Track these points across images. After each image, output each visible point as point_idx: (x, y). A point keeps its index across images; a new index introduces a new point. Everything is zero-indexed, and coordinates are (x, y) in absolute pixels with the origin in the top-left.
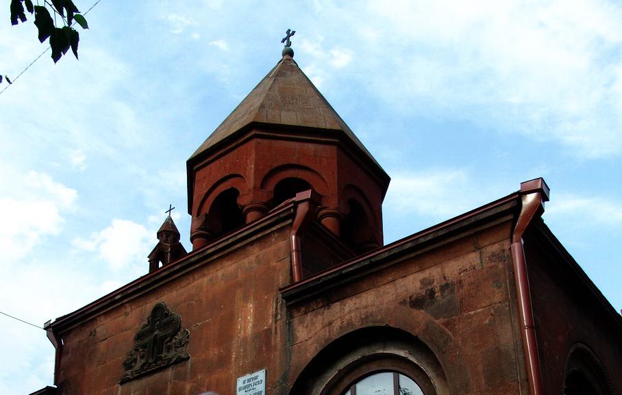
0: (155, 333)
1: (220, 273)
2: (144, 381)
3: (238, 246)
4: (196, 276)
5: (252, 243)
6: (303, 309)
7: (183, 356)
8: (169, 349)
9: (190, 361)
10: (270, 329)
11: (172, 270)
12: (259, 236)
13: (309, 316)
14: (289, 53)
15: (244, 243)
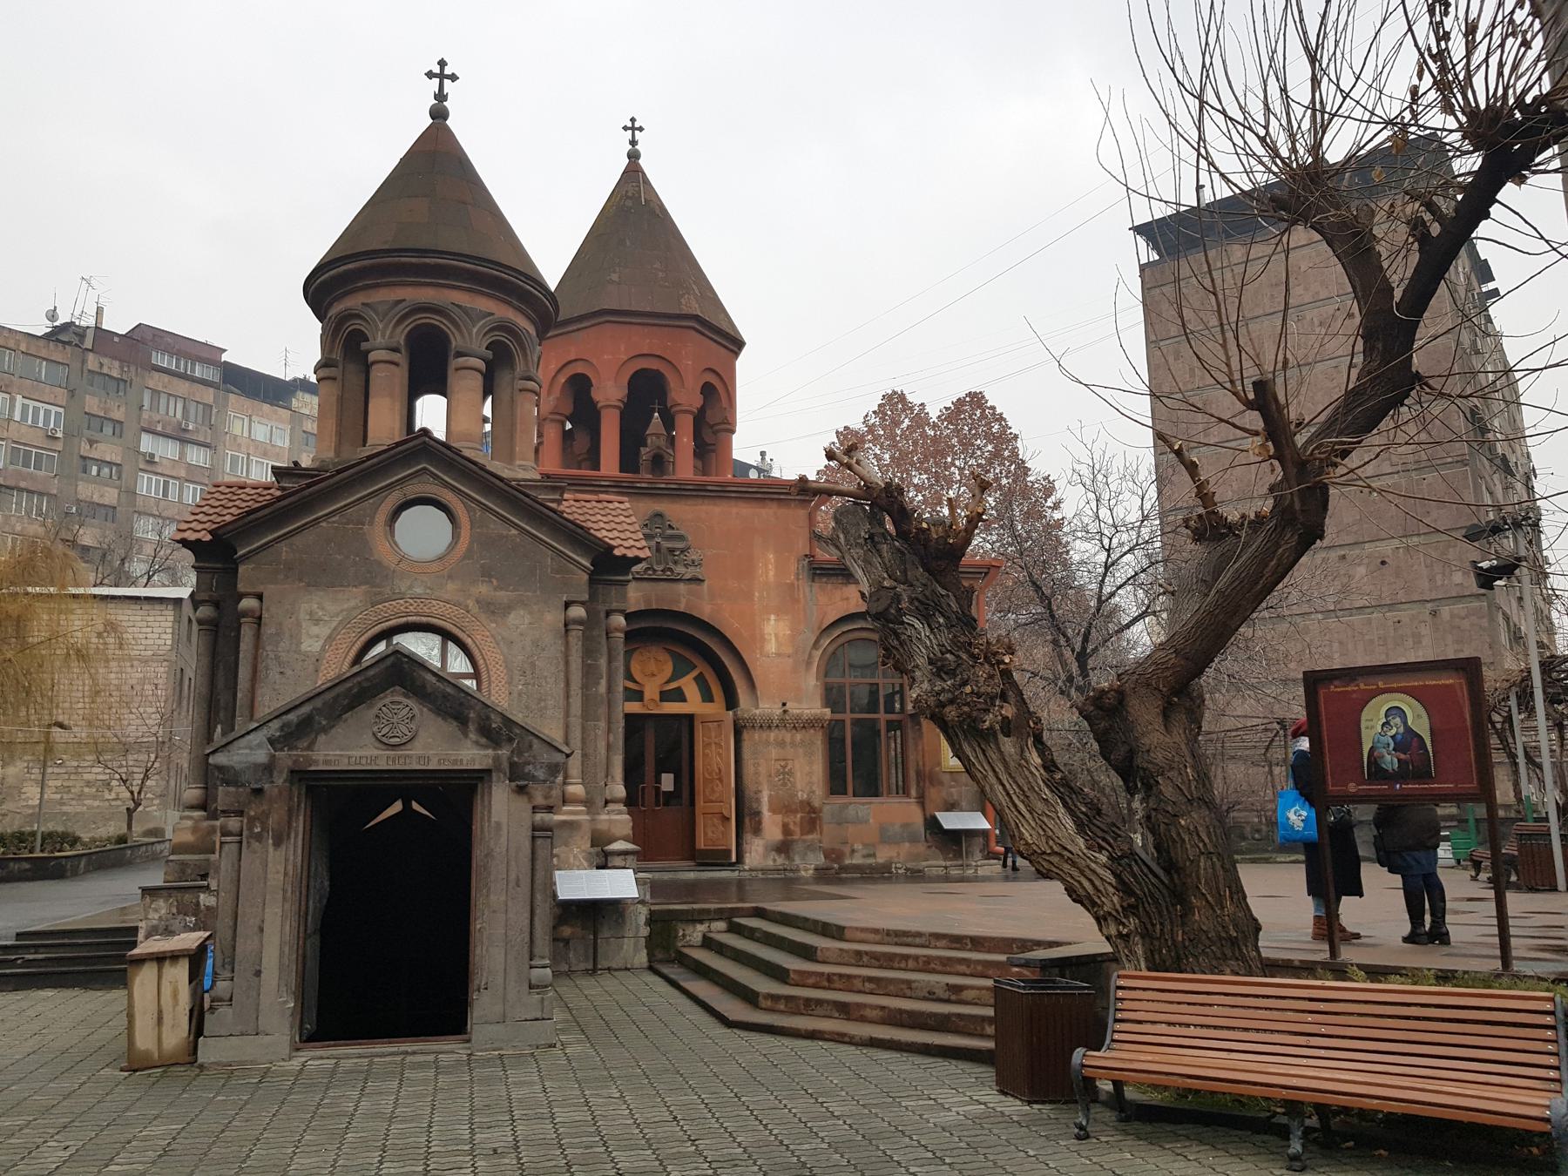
0: (656, 540)
1: (734, 510)
2: (645, 585)
3: (759, 496)
4: (706, 501)
5: (772, 499)
6: (824, 580)
7: (700, 577)
8: (676, 563)
9: (706, 583)
10: (793, 584)
11: (683, 487)
12: (782, 497)
13: (829, 586)
14: (634, 156)
15: (767, 496)
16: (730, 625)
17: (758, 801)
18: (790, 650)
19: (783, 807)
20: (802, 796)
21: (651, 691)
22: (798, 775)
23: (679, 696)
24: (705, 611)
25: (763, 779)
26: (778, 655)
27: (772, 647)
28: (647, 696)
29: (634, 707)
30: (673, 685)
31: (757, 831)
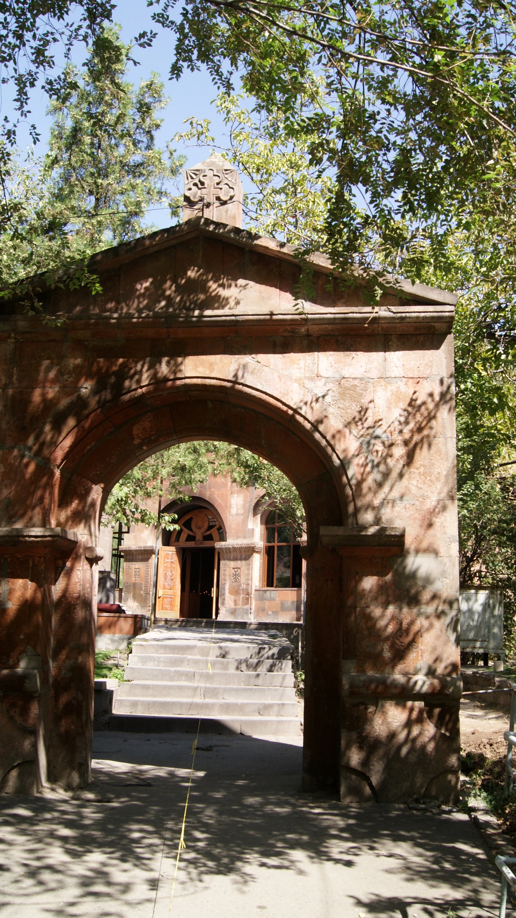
16: (218, 502)
17: (224, 589)
18: (241, 511)
19: (235, 592)
20: (244, 586)
21: (199, 536)
22: (242, 576)
23: (210, 538)
24: (207, 496)
25: (227, 578)
26: (237, 515)
27: (234, 511)
28: (197, 539)
29: (191, 544)
30: (208, 533)
31: (223, 604)
